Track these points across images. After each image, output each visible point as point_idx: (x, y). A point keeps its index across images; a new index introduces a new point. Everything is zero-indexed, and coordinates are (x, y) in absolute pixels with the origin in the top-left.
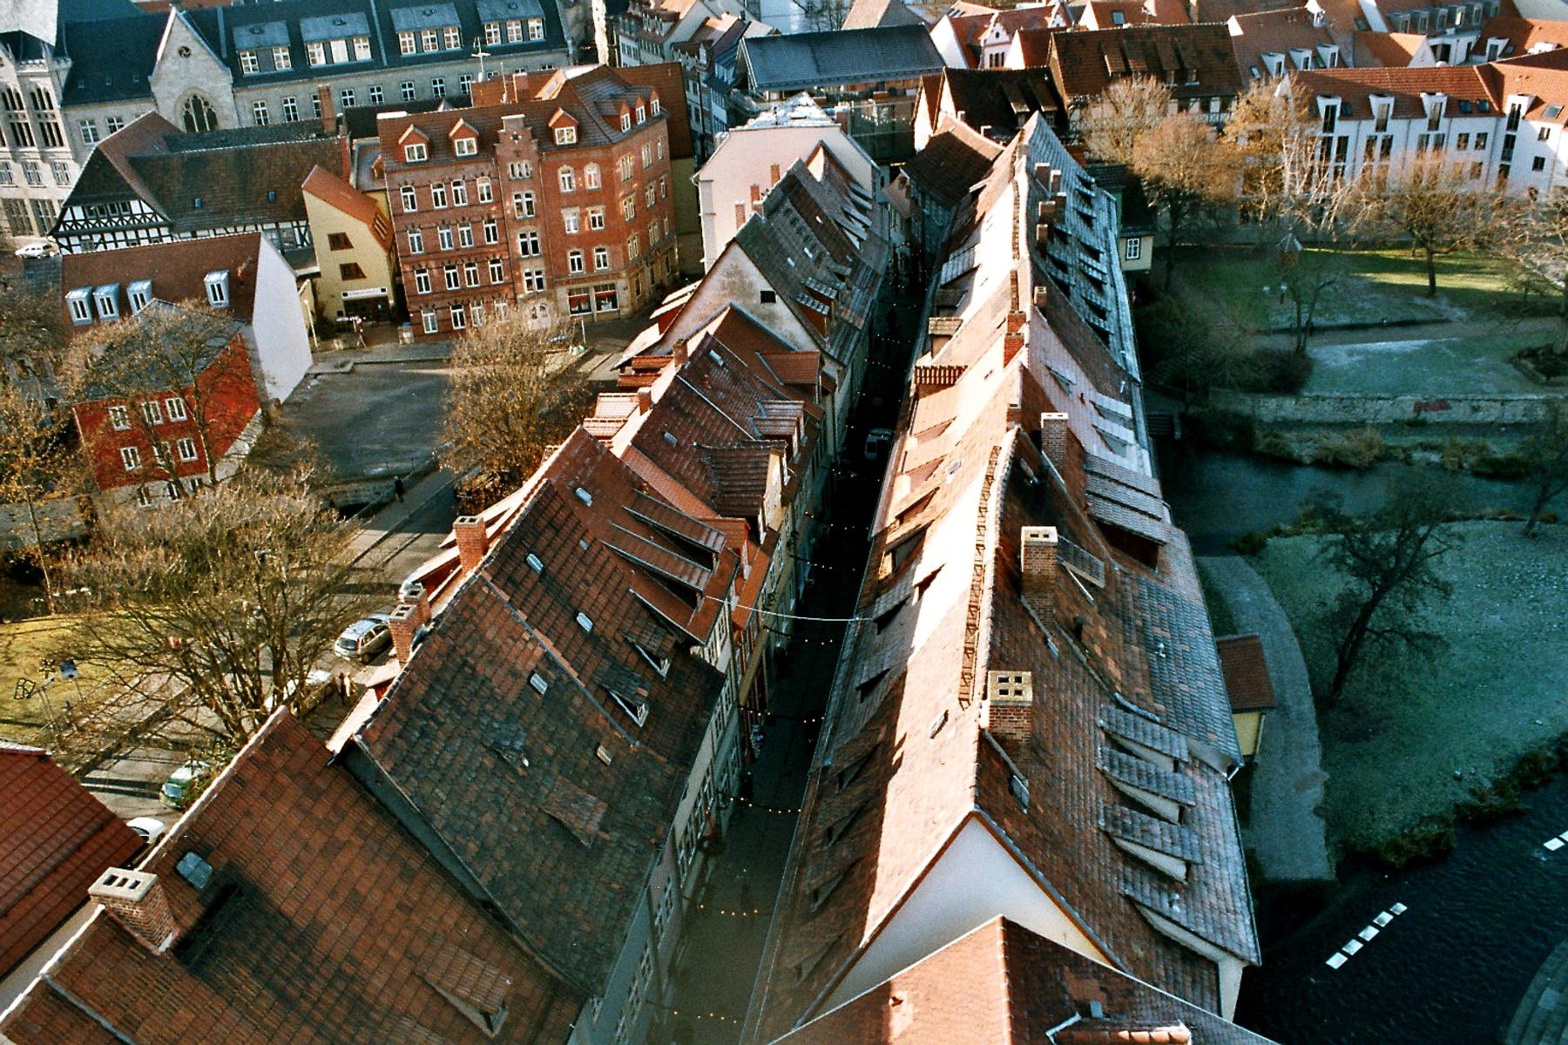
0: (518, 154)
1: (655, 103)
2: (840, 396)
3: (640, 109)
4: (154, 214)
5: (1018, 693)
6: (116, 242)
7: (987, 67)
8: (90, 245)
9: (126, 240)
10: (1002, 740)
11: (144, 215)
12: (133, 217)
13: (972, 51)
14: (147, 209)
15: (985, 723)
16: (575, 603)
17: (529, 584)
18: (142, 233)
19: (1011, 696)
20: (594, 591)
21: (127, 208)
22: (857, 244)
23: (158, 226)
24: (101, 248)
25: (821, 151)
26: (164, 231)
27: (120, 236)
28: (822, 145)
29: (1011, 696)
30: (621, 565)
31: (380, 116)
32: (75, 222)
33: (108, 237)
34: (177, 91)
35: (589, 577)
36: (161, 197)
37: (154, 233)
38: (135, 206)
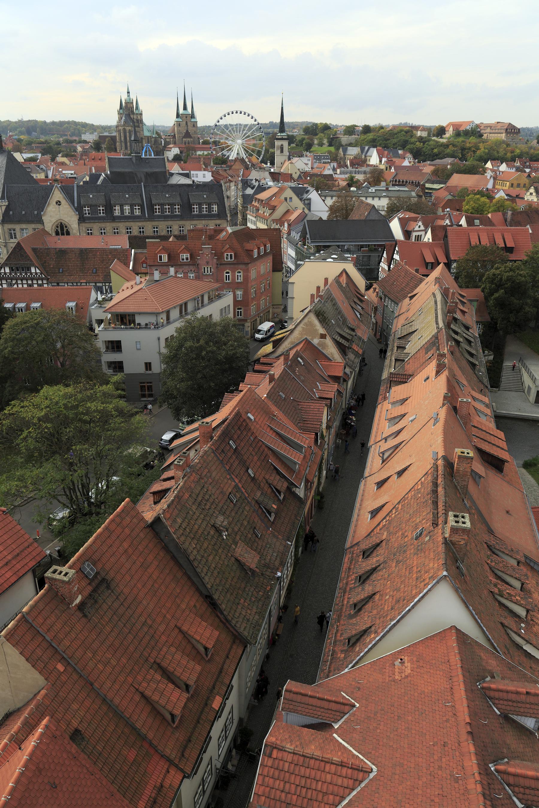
0: (208, 263)
1: (268, 246)
2: (350, 383)
3: (262, 248)
4: (41, 273)
5: (464, 523)
6: (22, 284)
7: (413, 240)
8: (11, 285)
9: (27, 284)
10: (453, 544)
11: (36, 273)
12: (31, 274)
13: (407, 234)
14: (38, 271)
15: (447, 535)
16: (248, 464)
17: (229, 454)
18: (35, 282)
19: (460, 524)
20: (256, 458)
21: (29, 269)
22: (359, 316)
23: (42, 280)
24: (15, 286)
25: (344, 275)
26: (45, 282)
27: (25, 282)
28: (344, 271)
29: (460, 524)
30: (266, 449)
31: (147, 240)
32: (5, 273)
33: (19, 282)
34: (54, 220)
35: (254, 453)
36: (44, 266)
37: (40, 282)
38: (33, 270)
